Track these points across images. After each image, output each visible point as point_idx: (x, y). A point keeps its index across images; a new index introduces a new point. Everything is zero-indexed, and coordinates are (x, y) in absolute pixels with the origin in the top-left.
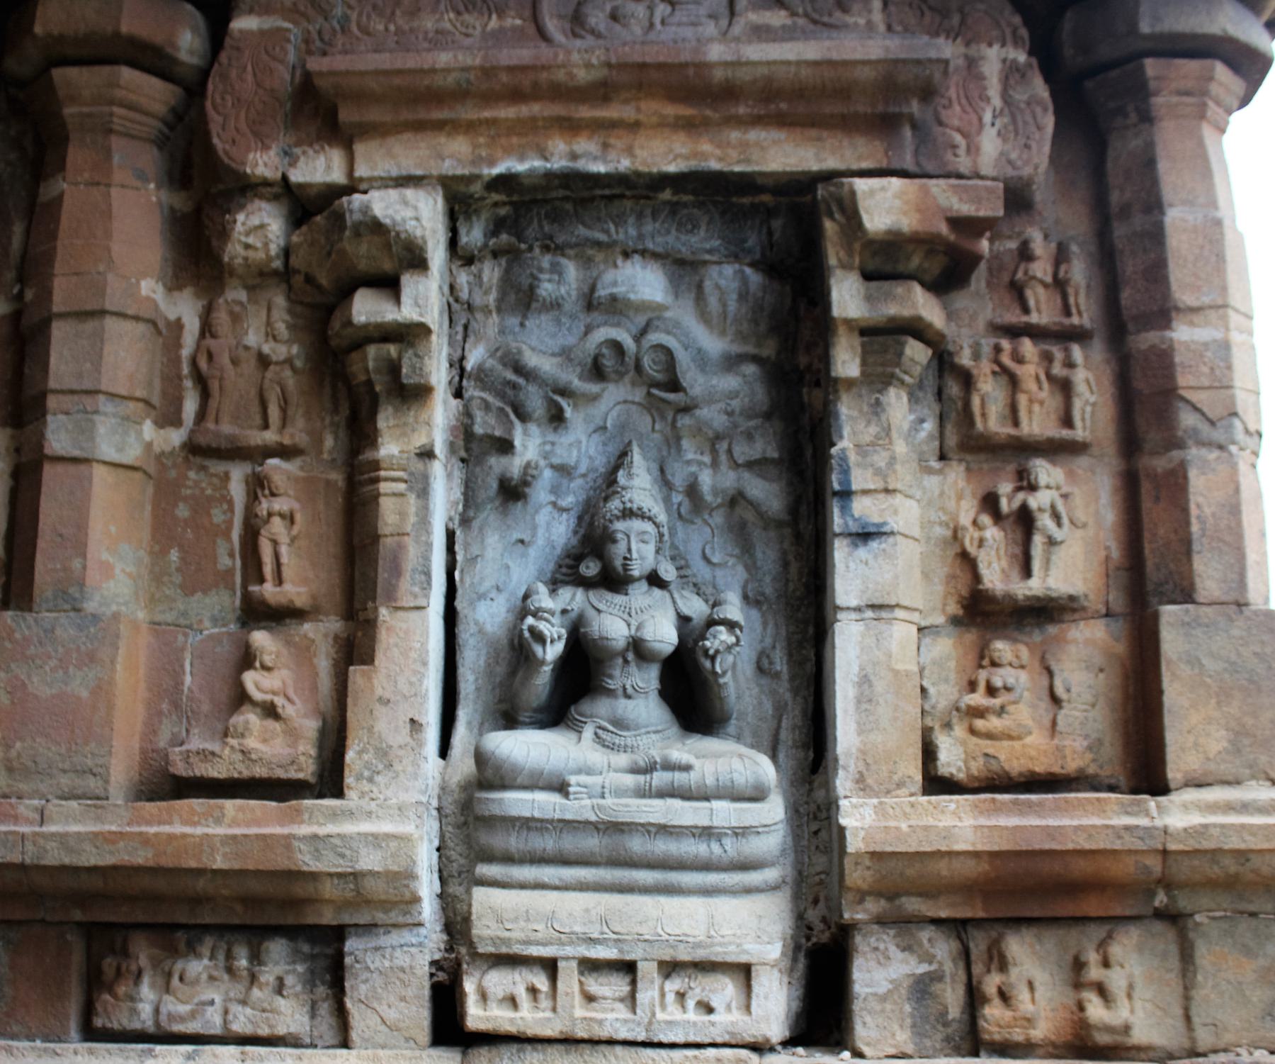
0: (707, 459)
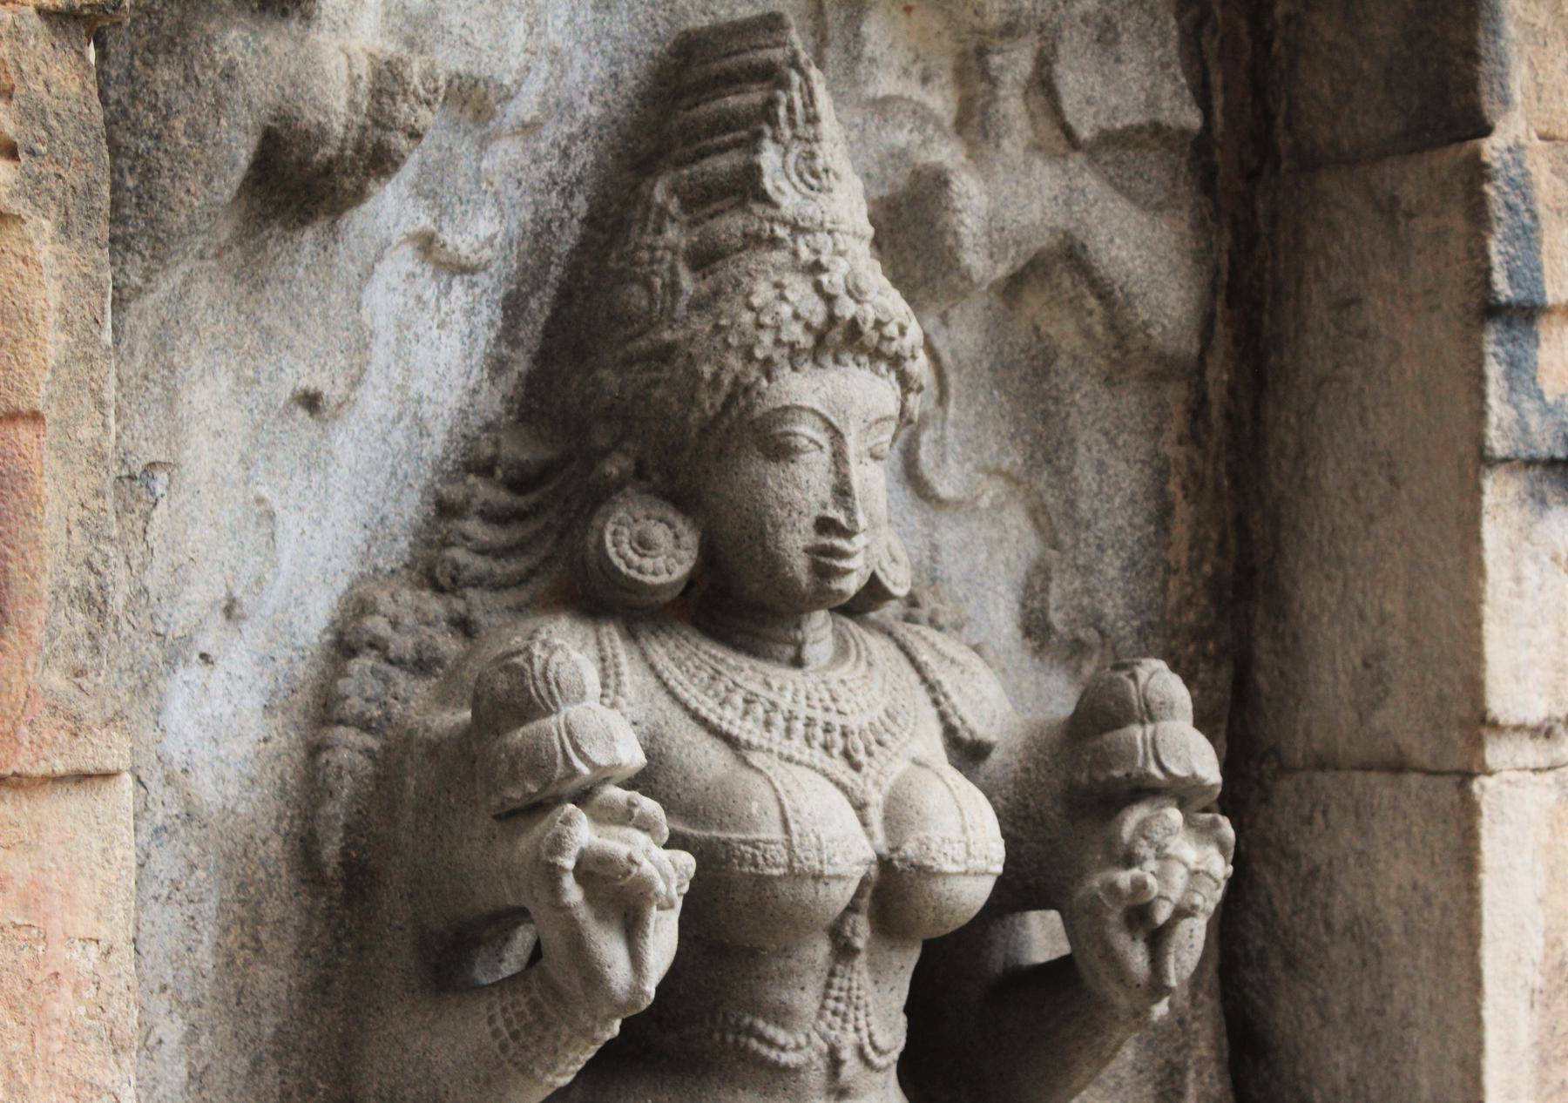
0: (941, 101)
